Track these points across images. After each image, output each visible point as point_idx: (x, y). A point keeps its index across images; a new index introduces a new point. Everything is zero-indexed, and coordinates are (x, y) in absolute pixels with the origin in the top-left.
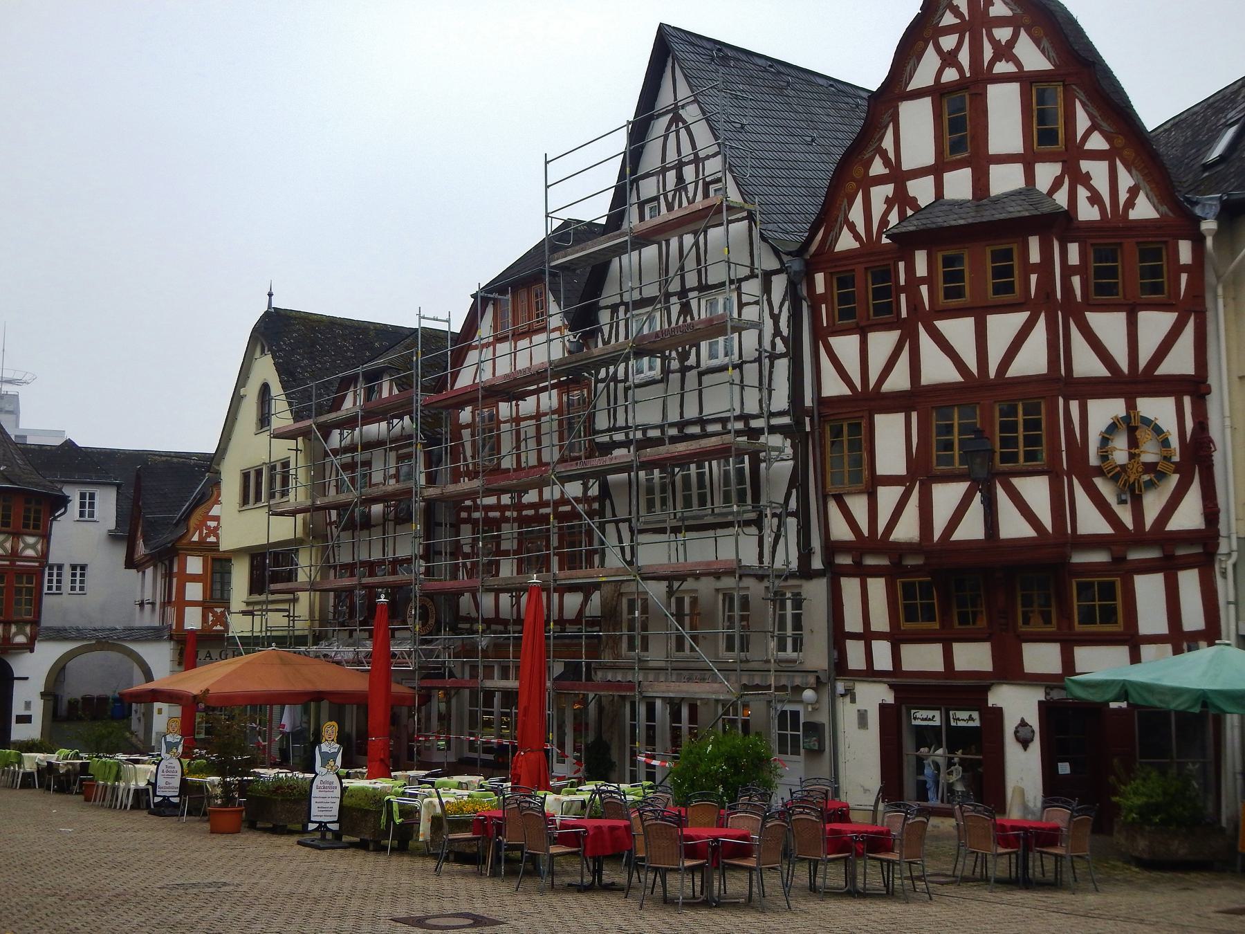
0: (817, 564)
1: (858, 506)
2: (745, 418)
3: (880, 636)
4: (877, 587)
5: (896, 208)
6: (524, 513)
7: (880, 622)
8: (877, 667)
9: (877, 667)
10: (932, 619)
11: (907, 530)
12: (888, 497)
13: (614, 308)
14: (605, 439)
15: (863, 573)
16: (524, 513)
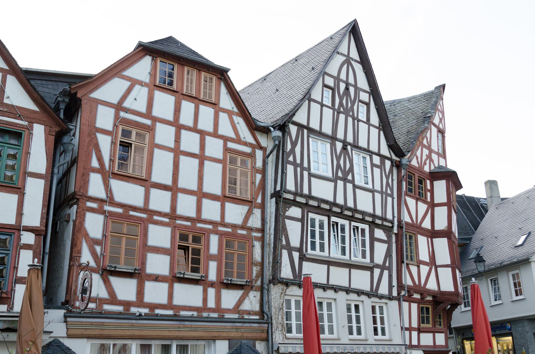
0: (395, 293)
1: (414, 269)
2: (374, 216)
3: (414, 329)
4: (414, 306)
5: (429, 160)
6: (178, 222)
7: (415, 324)
8: (413, 344)
9: (413, 344)
10: (428, 323)
11: (432, 285)
12: (424, 269)
13: (300, 126)
14: (291, 197)
15: (410, 299)
16: (178, 222)
